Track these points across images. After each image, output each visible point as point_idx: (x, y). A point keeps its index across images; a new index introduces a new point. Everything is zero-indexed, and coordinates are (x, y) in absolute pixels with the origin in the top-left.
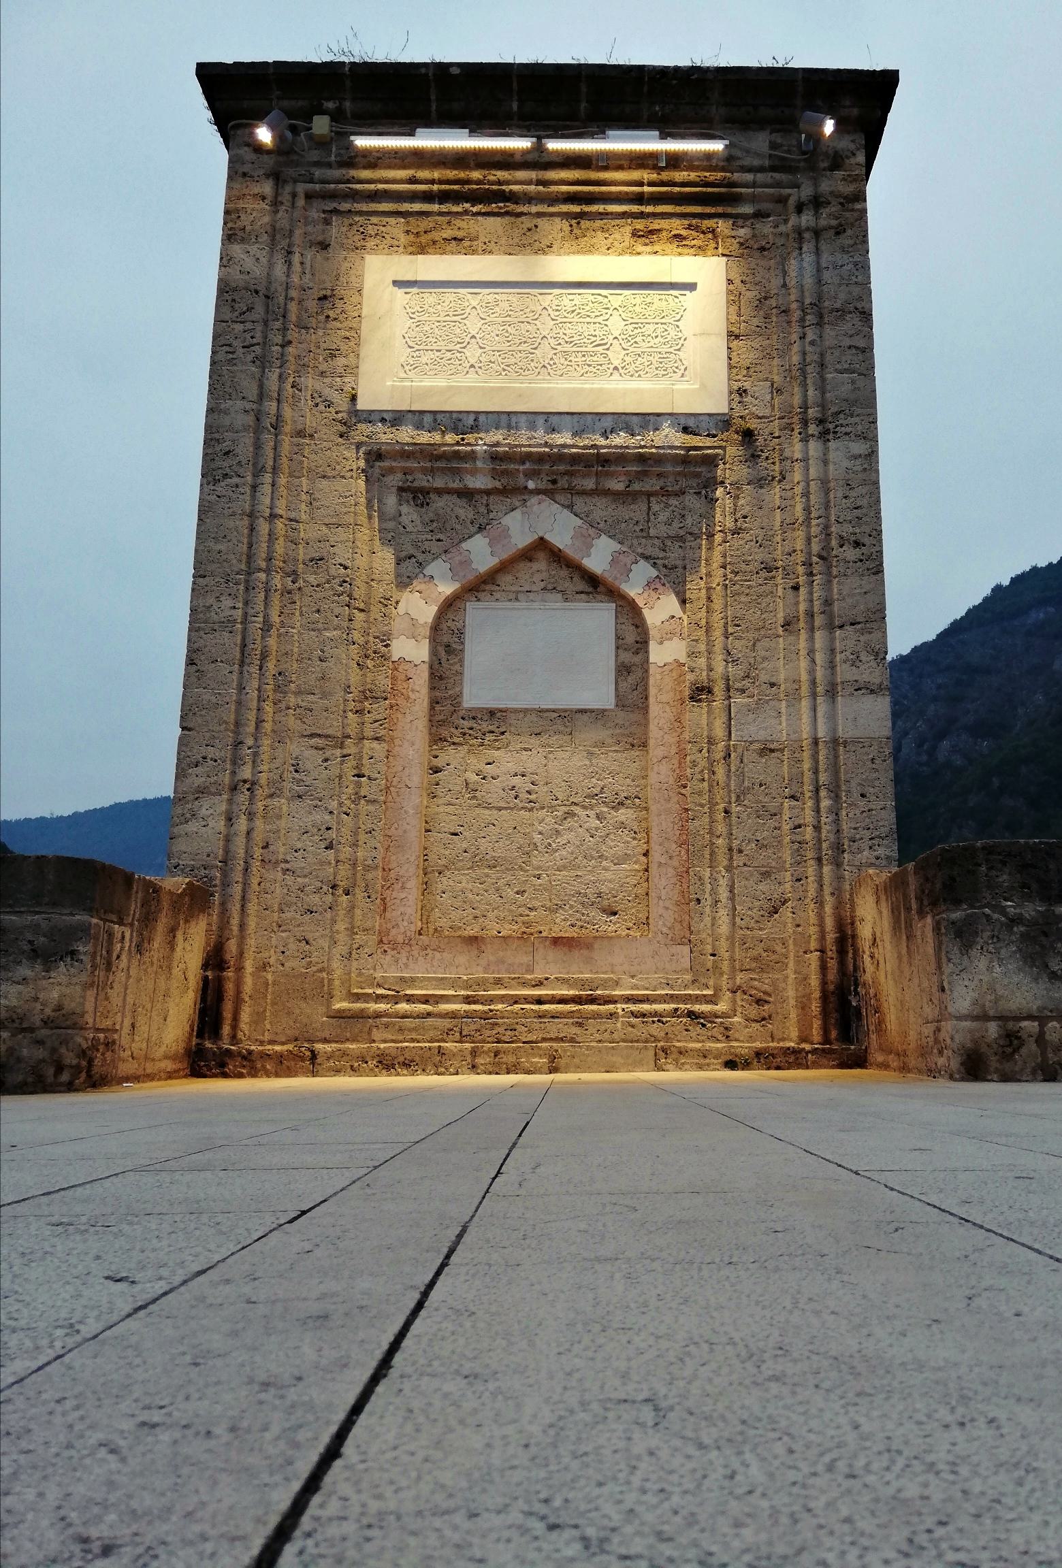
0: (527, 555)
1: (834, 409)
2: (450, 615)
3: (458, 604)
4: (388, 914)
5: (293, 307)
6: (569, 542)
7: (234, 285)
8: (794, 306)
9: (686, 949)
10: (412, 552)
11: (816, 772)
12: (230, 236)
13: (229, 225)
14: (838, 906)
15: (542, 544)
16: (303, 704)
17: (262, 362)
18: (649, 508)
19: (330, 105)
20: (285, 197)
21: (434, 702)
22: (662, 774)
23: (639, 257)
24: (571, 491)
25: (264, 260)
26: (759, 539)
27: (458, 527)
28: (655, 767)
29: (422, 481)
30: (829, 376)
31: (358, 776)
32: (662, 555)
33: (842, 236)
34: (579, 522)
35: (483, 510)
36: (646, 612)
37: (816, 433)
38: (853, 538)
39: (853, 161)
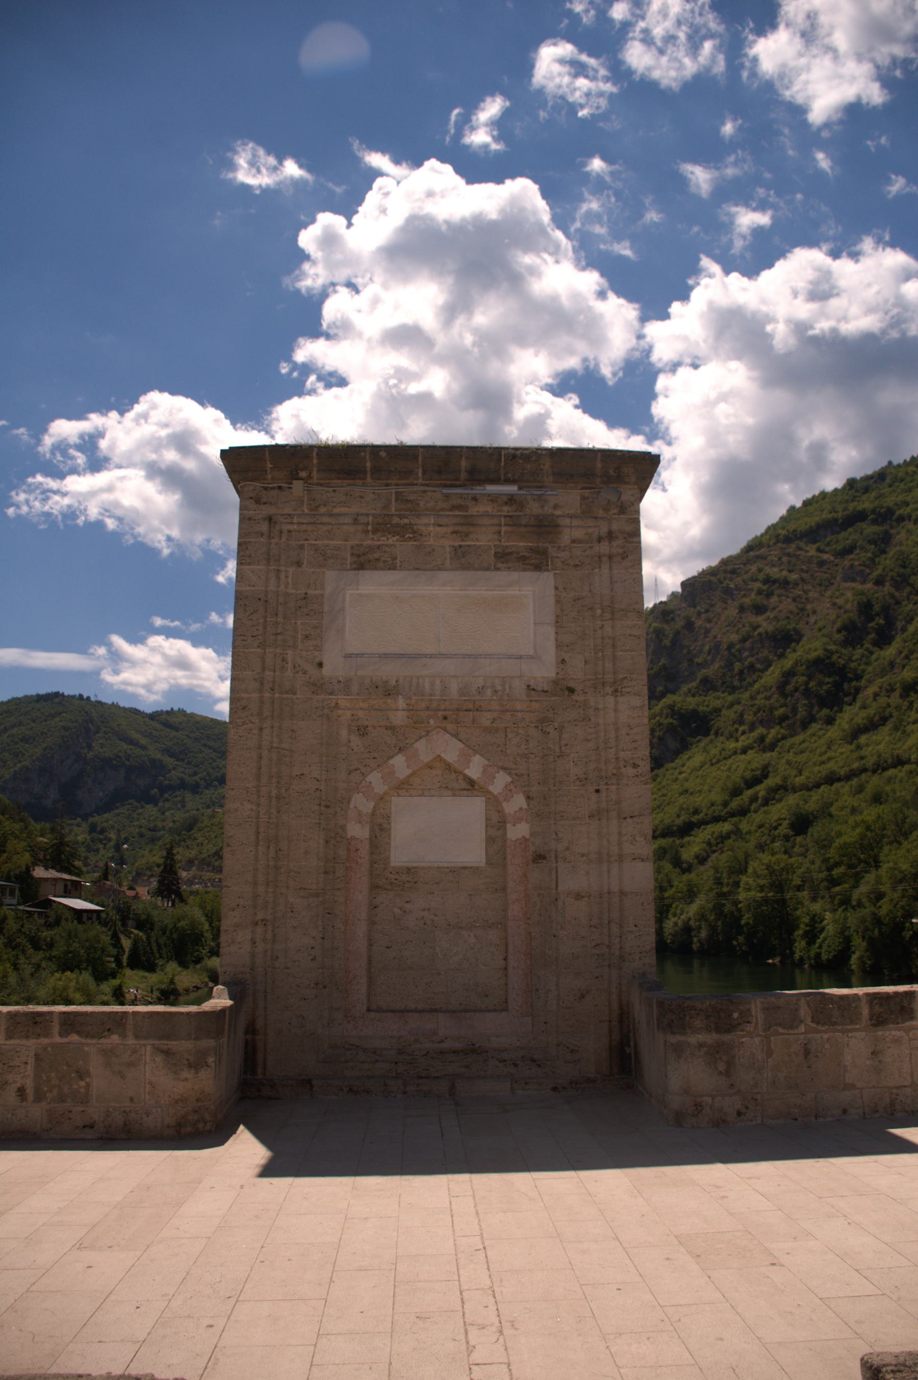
1: (621, 676)
6: (456, 759)
13: (242, 553)
17: (262, 645)
18: (506, 736)
21: (373, 862)
23: (499, 573)
26: (575, 759)
34: (462, 746)
36: (504, 804)
37: (610, 692)
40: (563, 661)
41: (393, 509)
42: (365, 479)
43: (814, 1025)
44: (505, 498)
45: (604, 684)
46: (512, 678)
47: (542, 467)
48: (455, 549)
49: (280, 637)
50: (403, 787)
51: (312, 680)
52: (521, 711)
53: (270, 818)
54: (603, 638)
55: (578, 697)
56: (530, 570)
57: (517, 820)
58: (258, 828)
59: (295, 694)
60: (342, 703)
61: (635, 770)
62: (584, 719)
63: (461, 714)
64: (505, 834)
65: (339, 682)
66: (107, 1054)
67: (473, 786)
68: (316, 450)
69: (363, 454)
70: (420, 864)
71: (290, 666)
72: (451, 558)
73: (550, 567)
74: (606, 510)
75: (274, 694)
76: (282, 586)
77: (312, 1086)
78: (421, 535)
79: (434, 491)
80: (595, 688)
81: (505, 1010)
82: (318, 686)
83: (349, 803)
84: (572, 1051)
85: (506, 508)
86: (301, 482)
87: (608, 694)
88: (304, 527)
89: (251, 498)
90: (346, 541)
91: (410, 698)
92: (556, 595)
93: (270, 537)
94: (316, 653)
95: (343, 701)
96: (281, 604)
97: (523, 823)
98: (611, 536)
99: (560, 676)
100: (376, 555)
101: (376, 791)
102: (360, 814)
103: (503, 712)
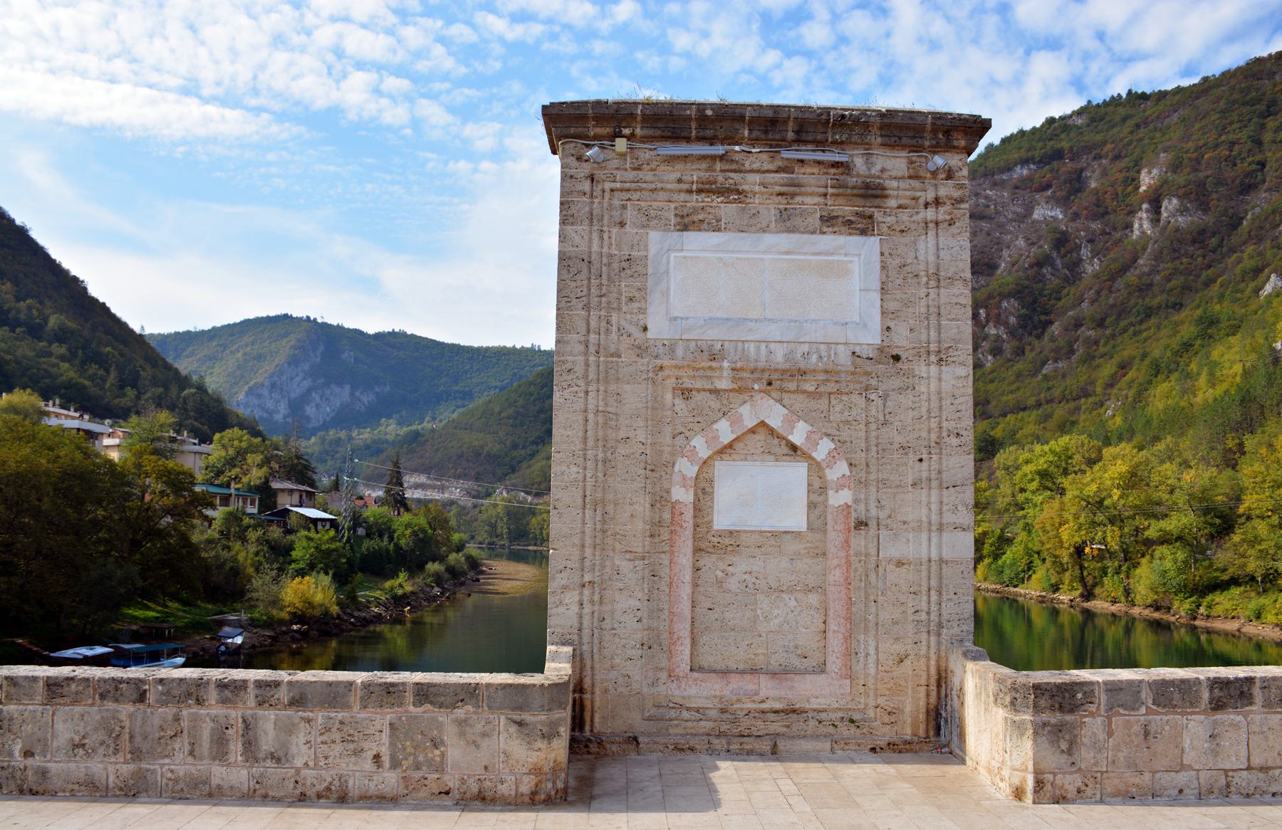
0: (752, 431)
1: (947, 345)
2: (705, 469)
3: (710, 462)
4: (673, 660)
5: (604, 269)
7: (568, 255)
8: (922, 273)
9: (848, 682)
10: (682, 430)
11: (929, 579)
12: (563, 222)
13: (564, 213)
14: (939, 657)
15: (763, 424)
17: (587, 307)
19: (626, 131)
20: (597, 192)
21: (696, 526)
22: (836, 575)
23: (825, 237)
24: (782, 390)
25: (586, 238)
29: (688, 384)
30: (943, 322)
32: (837, 433)
33: (953, 227)
34: (786, 411)
35: (725, 402)
36: (827, 471)
39: (960, 174)
43: (1154, 707)
49: (604, 299)
50: (726, 450)
53: (596, 481)
57: (839, 487)
58: (585, 491)
59: (620, 357)
64: (827, 500)
65: (664, 345)
70: (742, 529)
71: (614, 329)
76: (605, 250)
77: (638, 743)
81: (823, 671)
82: (641, 350)
84: (889, 713)
86: (625, 140)
92: (882, 261)
93: (592, 196)
94: (641, 316)
97: (846, 490)
98: (937, 202)
100: (701, 217)
101: (700, 455)
102: (684, 478)
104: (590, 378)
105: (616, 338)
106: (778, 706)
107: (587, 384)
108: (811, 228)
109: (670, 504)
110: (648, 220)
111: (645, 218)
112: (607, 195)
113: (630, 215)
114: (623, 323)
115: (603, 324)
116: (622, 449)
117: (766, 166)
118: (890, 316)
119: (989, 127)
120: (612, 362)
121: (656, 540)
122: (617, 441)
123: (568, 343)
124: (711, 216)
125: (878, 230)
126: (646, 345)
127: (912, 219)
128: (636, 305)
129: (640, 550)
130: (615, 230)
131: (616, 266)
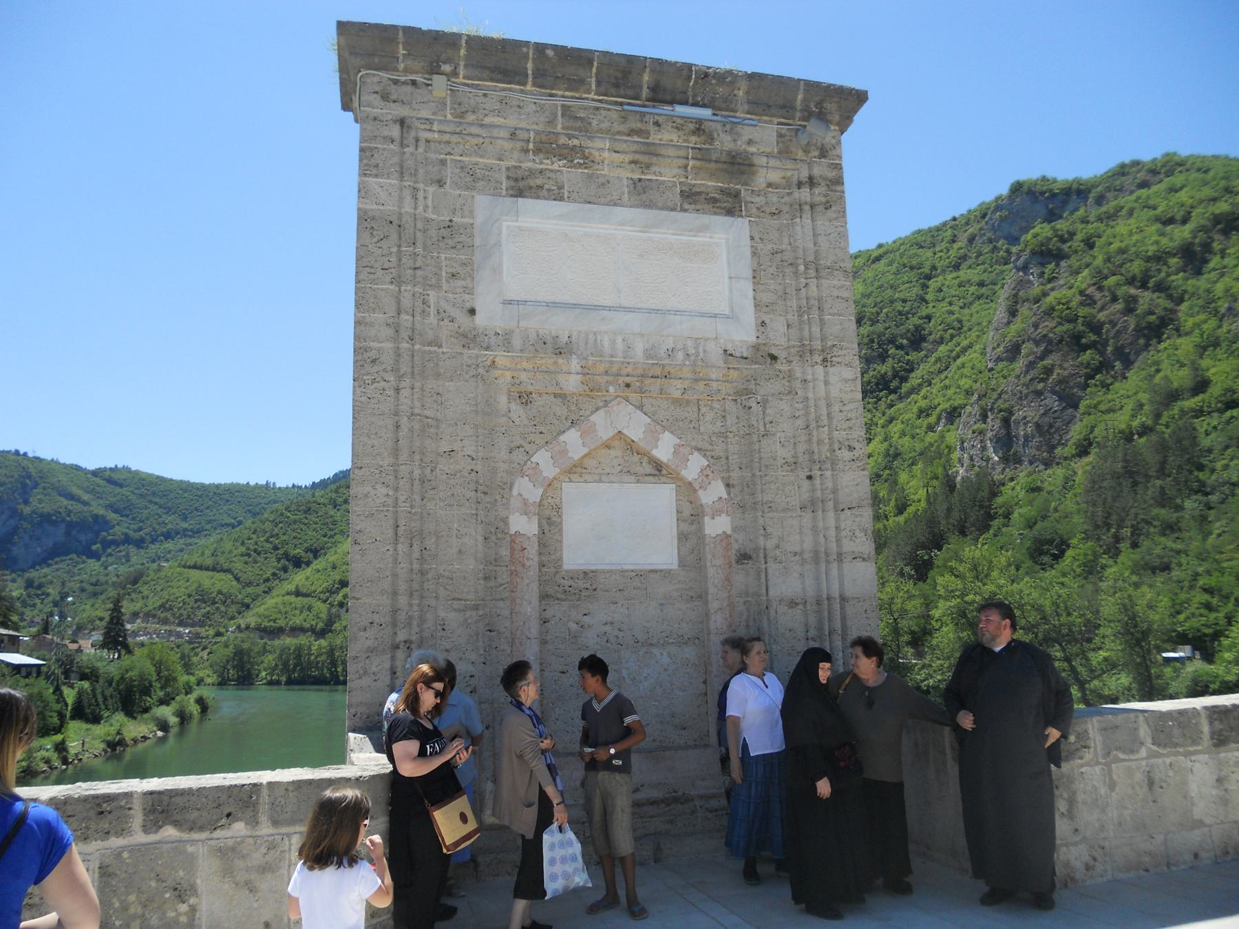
1: (830, 344)
2: (550, 493)
5: (419, 235)
7: (370, 214)
10: (519, 441)
12: (363, 173)
13: (365, 162)
16: (446, 574)
17: (398, 281)
26: (782, 440)
27: (556, 422)
28: (713, 618)
31: (490, 631)
32: (710, 447)
34: (649, 420)
35: (573, 408)
36: (701, 492)
38: (847, 443)
40: (763, 324)
41: (560, 126)
42: (524, 84)
43: (1155, 748)
44: (692, 126)
45: (811, 352)
46: (706, 340)
47: (736, 92)
48: (635, 183)
49: (419, 273)
50: (575, 470)
51: (462, 329)
52: (717, 381)
54: (807, 299)
55: (782, 366)
56: (721, 214)
58: (396, 520)
59: (440, 346)
60: (501, 361)
61: (851, 454)
62: (790, 392)
63: (648, 381)
64: (701, 528)
66: (227, 854)
67: (660, 471)
68: (465, 38)
69: (525, 50)
70: (599, 567)
71: (432, 310)
72: (629, 192)
73: (744, 213)
74: (806, 152)
75: (413, 345)
76: (421, 209)
78: (593, 161)
79: (609, 110)
80: (801, 356)
82: (469, 339)
83: (511, 490)
85: (693, 139)
87: (817, 363)
88: (446, 137)
89: (377, 93)
90: (500, 159)
91: (586, 359)
92: (752, 246)
93: (402, 145)
95: (502, 359)
96: (420, 230)
98: (812, 182)
99: (760, 341)
100: (539, 182)
101: (545, 474)
102: (525, 502)
103: (696, 380)
104: (402, 372)
105: (435, 322)
106: (656, 794)
107: (400, 378)
108: (670, 204)
109: (508, 539)
110: (473, 179)
111: (469, 179)
112: (422, 144)
113: (450, 172)
114: (443, 304)
115: (419, 303)
116: (444, 466)
117: (617, 127)
118: (765, 309)
119: (867, 99)
120: (430, 352)
121: (492, 584)
122: (439, 454)
123: (372, 324)
124: (551, 182)
125: (747, 210)
126: (474, 333)
127: (783, 200)
128: (459, 283)
129: (471, 596)
130: (432, 189)
131: (433, 232)
